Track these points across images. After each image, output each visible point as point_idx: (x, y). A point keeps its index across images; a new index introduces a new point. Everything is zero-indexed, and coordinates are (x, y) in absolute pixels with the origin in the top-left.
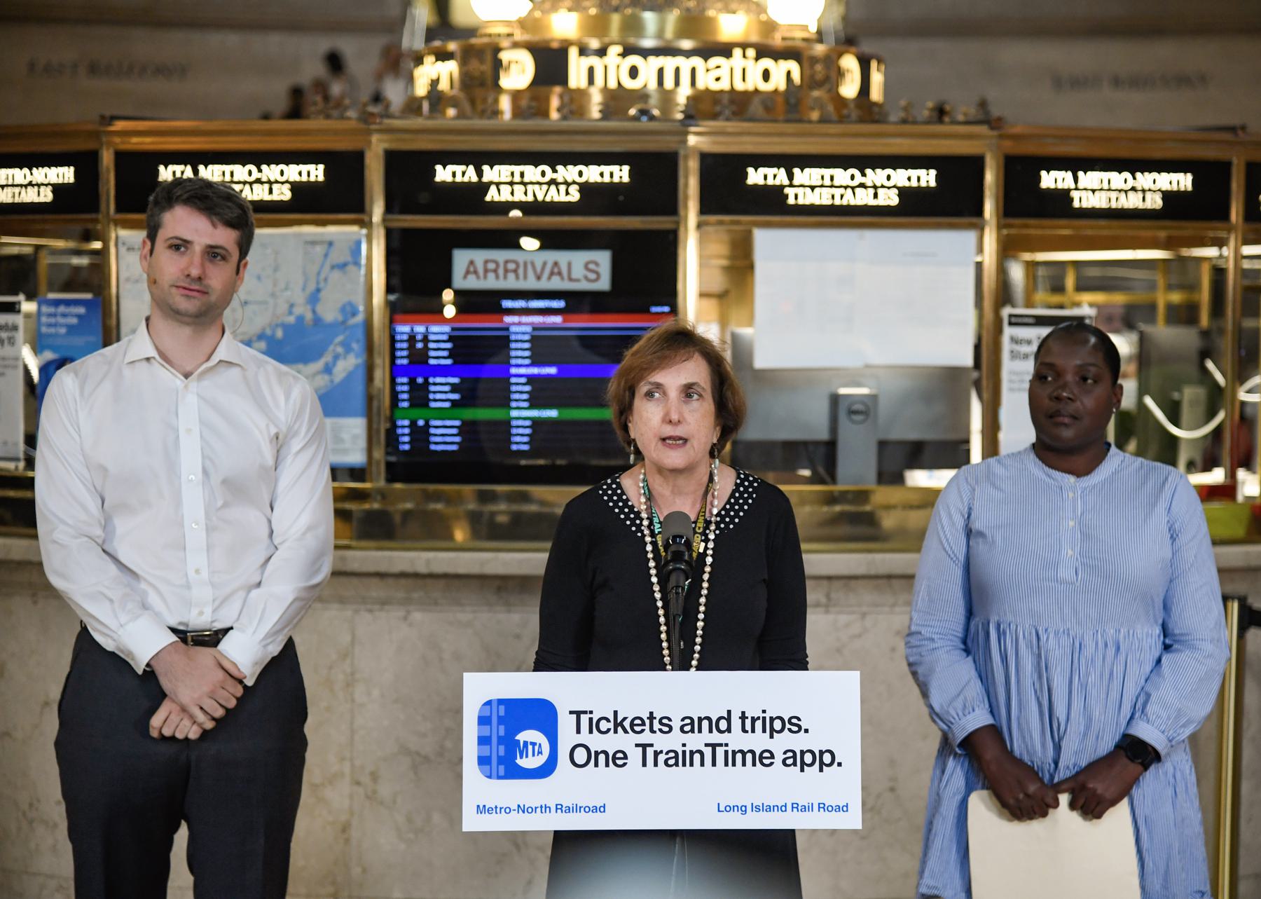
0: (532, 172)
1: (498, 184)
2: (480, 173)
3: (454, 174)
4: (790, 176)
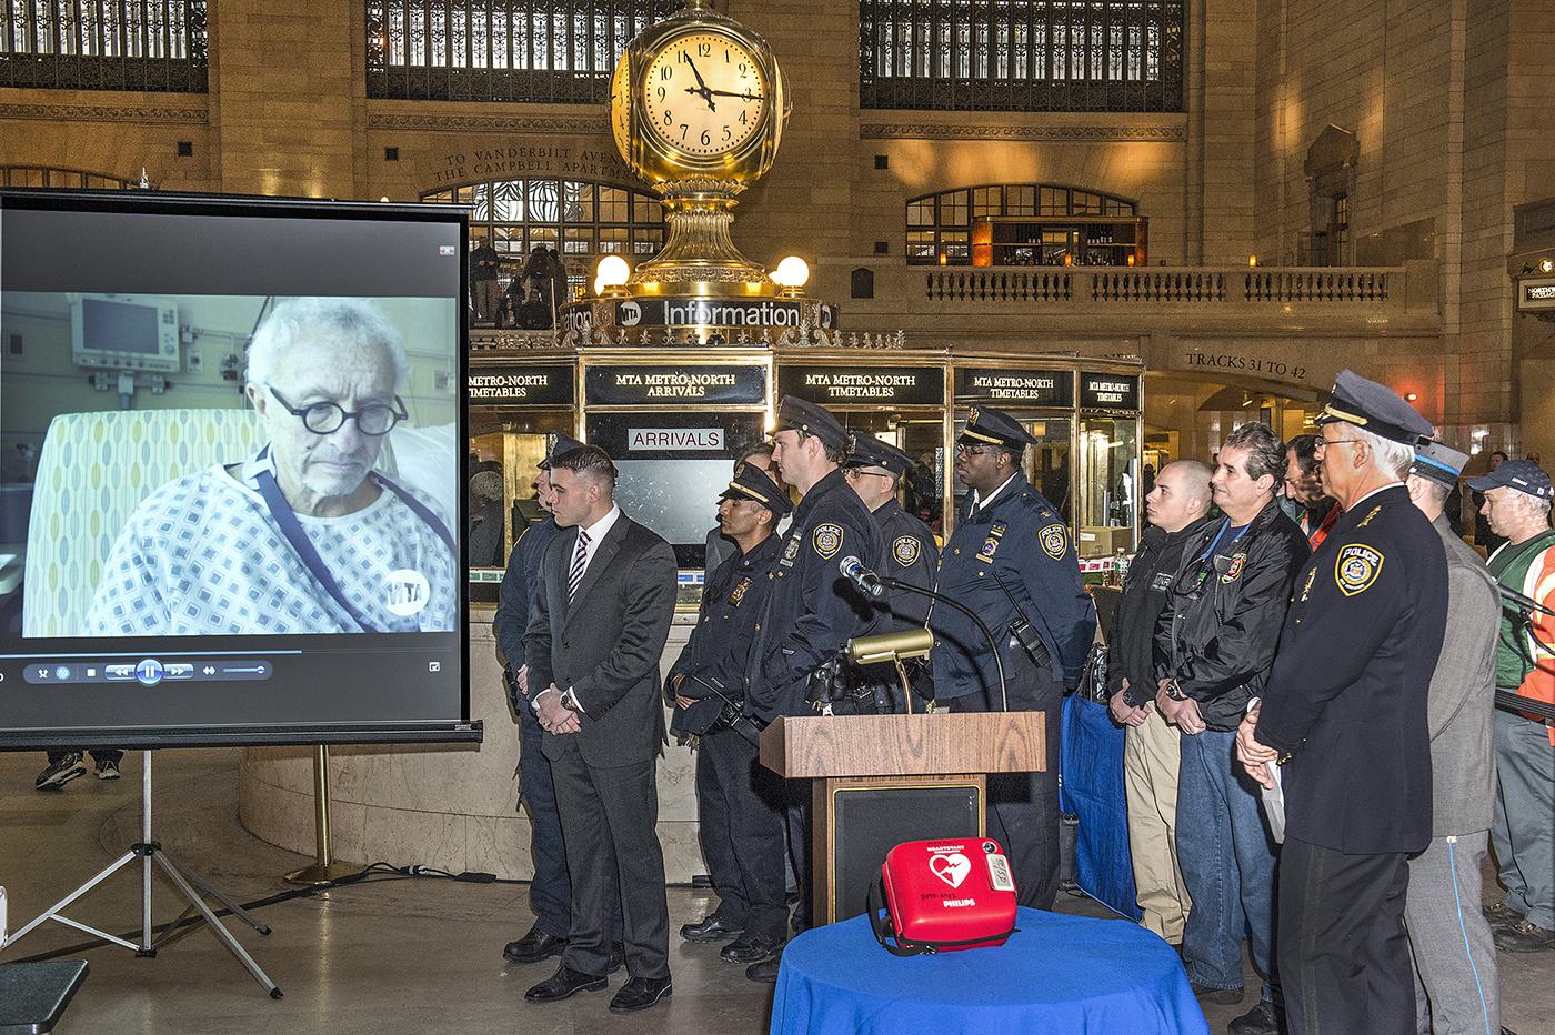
0: (675, 379)
1: (654, 387)
2: (644, 380)
3: (628, 380)
4: (832, 380)
